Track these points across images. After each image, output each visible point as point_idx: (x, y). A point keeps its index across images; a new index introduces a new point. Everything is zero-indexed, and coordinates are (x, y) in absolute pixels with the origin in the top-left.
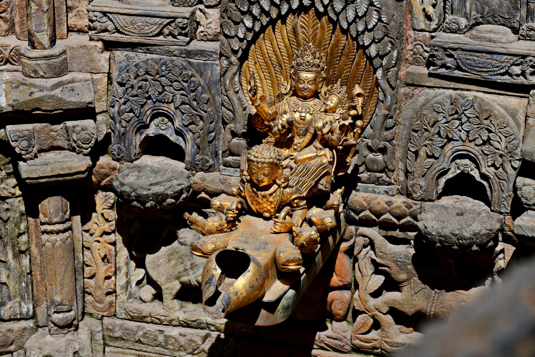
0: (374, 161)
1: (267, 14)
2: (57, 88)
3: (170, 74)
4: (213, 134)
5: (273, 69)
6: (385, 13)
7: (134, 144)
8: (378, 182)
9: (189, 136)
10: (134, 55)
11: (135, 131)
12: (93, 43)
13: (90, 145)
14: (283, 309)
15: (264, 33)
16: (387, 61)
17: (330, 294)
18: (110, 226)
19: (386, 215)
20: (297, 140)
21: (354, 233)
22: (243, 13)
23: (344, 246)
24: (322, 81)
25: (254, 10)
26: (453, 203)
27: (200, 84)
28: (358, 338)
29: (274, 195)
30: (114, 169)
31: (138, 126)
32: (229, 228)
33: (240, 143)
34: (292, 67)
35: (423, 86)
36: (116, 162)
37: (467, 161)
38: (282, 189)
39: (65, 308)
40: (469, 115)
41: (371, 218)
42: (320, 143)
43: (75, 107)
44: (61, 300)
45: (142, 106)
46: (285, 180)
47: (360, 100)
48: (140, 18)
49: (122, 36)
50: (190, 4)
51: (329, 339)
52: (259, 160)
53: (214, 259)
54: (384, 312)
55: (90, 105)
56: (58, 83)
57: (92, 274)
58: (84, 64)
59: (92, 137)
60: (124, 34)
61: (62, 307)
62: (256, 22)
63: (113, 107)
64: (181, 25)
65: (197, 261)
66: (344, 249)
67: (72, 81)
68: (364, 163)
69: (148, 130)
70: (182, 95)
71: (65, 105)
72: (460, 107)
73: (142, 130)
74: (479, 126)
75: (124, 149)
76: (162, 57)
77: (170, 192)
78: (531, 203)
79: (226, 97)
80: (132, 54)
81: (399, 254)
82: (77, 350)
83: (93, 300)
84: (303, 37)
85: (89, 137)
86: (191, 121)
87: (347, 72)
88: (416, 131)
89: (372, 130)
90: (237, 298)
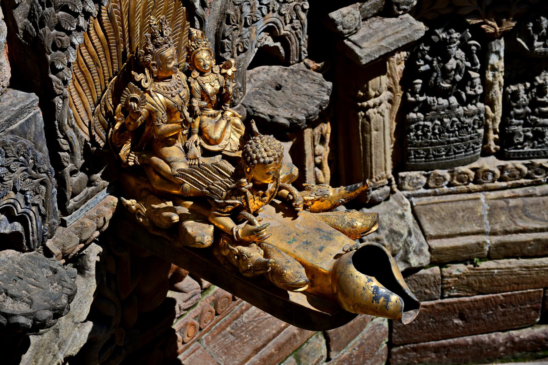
5: (89, 74)
9: (32, 212)
34: (147, 53)
42: (214, 109)
79: (62, 140)
88: (228, 38)
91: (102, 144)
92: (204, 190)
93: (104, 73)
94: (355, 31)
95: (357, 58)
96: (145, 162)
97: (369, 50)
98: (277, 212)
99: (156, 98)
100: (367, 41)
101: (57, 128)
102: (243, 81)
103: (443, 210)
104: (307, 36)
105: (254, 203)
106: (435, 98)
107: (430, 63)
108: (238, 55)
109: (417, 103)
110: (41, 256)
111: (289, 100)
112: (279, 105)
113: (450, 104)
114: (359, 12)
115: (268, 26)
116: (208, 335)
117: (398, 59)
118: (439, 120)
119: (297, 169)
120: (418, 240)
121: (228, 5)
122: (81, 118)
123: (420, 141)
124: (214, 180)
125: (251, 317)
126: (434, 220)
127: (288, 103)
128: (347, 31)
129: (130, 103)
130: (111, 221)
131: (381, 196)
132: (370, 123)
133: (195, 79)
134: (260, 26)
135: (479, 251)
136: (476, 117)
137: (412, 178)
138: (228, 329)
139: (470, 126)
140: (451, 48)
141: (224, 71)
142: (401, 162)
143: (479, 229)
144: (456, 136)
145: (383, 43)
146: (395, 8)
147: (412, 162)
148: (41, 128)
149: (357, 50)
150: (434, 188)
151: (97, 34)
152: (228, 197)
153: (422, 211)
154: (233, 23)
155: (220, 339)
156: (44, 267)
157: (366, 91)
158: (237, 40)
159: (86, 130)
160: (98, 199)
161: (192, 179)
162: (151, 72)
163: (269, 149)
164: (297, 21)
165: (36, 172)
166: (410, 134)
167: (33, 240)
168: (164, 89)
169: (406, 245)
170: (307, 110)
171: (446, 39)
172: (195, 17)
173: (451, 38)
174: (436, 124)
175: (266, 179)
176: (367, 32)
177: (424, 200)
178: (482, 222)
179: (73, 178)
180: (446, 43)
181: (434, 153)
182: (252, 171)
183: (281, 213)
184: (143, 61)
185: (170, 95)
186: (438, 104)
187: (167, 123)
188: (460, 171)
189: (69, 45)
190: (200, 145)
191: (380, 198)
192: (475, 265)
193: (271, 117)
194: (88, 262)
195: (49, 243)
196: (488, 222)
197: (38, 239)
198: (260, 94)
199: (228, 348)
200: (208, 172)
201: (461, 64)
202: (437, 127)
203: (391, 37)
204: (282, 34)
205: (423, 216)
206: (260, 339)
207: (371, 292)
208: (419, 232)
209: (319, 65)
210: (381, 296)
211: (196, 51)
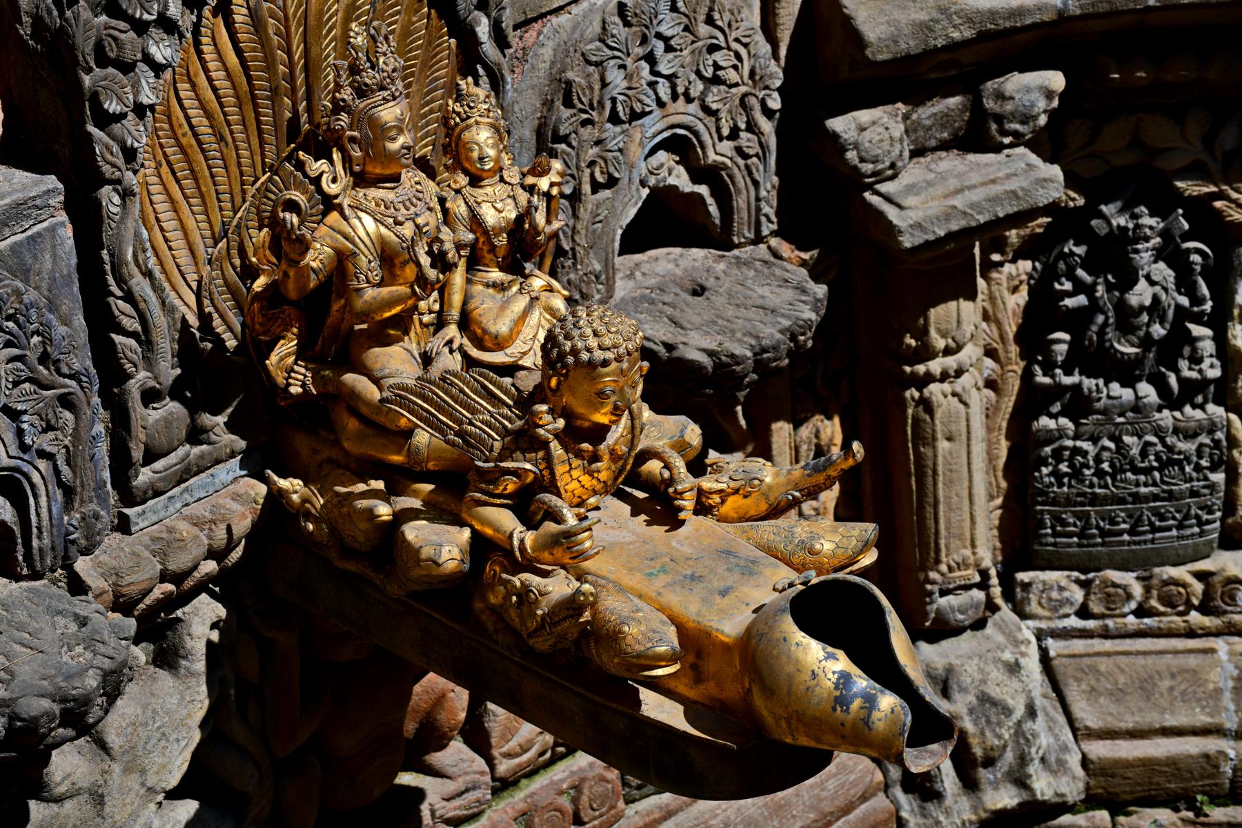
9: (39, 473)
17: (417, 688)
26: (631, 284)
28: (509, 755)
35: (543, 16)
37: (662, 156)
40: (669, 33)
42: (501, 270)
52: (622, 350)
53: (800, 636)
65: (117, 818)
72: (648, 24)
74: (690, 48)
78: (887, 164)
79: (120, 302)
88: (565, 139)
91: (231, 343)
92: (451, 437)
93: (239, 164)
94: (890, 172)
95: (891, 230)
96: (330, 389)
97: (921, 214)
98: (634, 513)
99: (355, 222)
100: (917, 194)
101: (108, 267)
102: (607, 259)
103: (1122, 671)
104: (775, 179)
105: (572, 478)
106: (1101, 382)
107: (1089, 290)
108: (594, 191)
109: (1058, 390)
110: (64, 593)
111: (717, 316)
112: (693, 324)
113: (1138, 398)
114: (902, 127)
115: (675, 135)
117: (1010, 277)
118: (1111, 438)
119: (698, 431)
120: (1056, 737)
121: (569, 60)
122: (178, 266)
123: (1065, 489)
124: (473, 411)
126: (1100, 694)
127: (715, 323)
128: (871, 166)
129: (281, 215)
130: (249, 537)
131: (962, 613)
132: (932, 418)
133: (458, 191)
134: (653, 130)
135: (1209, 777)
136: (1205, 439)
137: (1047, 587)
139: (1188, 459)
140: (1137, 251)
141: (530, 180)
142: (1022, 545)
143: (1209, 720)
144: (1155, 484)
145: (958, 202)
146: (994, 127)
147: (1047, 545)
148: (68, 266)
149: (892, 213)
150: (1102, 617)
151: (221, 58)
152: (506, 454)
153: (1070, 671)
154: (580, 106)
156: (59, 613)
157: (922, 334)
158: (592, 152)
159: (191, 299)
160: (217, 480)
161: (422, 408)
162: (347, 160)
163: (604, 331)
164: (750, 135)
165: (48, 369)
166: (1040, 471)
167: (40, 549)
168: (377, 205)
169: (1022, 741)
170: (757, 337)
171: (1123, 230)
172: (479, 67)
173: (1137, 226)
174: (1104, 448)
175: (597, 410)
176: (921, 179)
177: (1079, 645)
178: (1217, 706)
179: (151, 412)
180: (1125, 241)
181: (1102, 524)
182: (564, 387)
183: (643, 517)
184: (329, 129)
185: (391, 220)
186: (1109, 397)
187: (379, 285)
188: (1165, 577)
189: (139, 56)
190: (461, 348)
191: (960, 617)
192: (1199, 812)
193: (669, 347)
194: (187, 639)
195: (82, 565)
196: (1232, 707)
197: (53, 549)
198: (652, 302)
200: (462, 391)
201: (1164, 296)
202: (1106, 455)
203: (977, 190)
204: (710, 161)
205: (1071, 681)
207: (830, 684)
208: (1062, 719)
209: (806, 256)
210: (856, 696)
211: (462, 125)
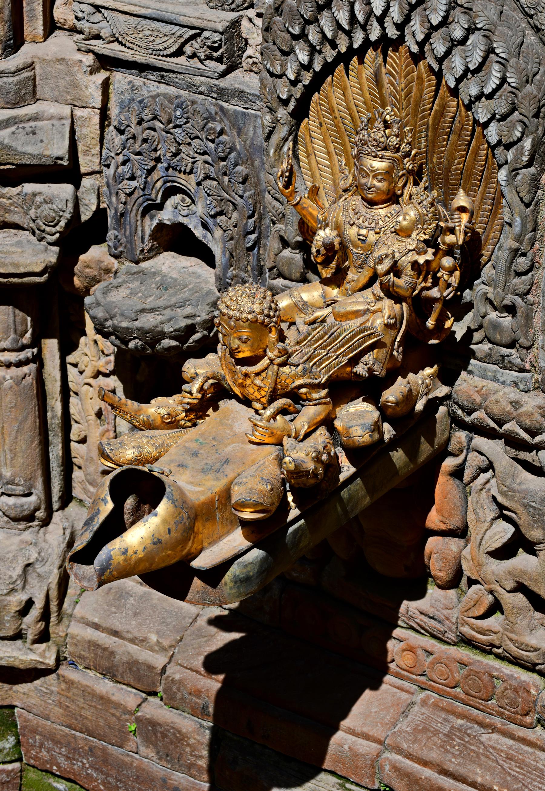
0: (496, 326)
1: (334, 45)
2: (6, 127)
3: (189, 125)
4: (253, 237)
6: (513, 70)
7: (140, 233)
8: (504, 363)
10: (141, 83)
11: (140, 212)
12: (79, 56)
13: (58, 228)
14: (235, 582)
15: (333, 76)
16: (515, 156)
18: (108, 363)
19: (511, 424)
20: (351, 275)
21: (465, 444)
22: (295, 38)
23: (449, 463)
24: (403, 175)
25: (310, 34)
27: (232, 149)
29: (264, 375)
30: (108, 271)
31: (145, 204)
32: (189, 421)
33: (293, 259)
36: (113, 260)
38: (276, 367)
39: (19, 490)
41: (488, 425)
43: (34, 162)
44: (12, 475)
45: (150, 172)
46: (280, 352)
47: (465, 217)
48: (149, 22)
49: (123, 48)
50: (233, 6)
51: (422, 617)
52: (231, 313)
54: (508, 589)
55: (60, 162)
56: (8, 120)
57: (82, 436)
58: (61, 89)
59: (61, 217)
60: (125, 45)
61: (14, 487)
62: (316, 54)
63: (108, 166)
64: (209, 43)
66: (449, 469)
67: (36, 118)
68: (481, 327)
69: (162, 212)
70: (206, 162)
71: (17, 157)
73: (153, 212)
75: (123, 240)
76: (182, 92)
77: (168, 328)
80: (138, 81)
81: (532, 494)
82: (31, 561)
83: (84, 478)
84: (391, 91)
85: (54, 215)
86: (218, 209)
87: (459, 164)
89: (494, 271)
90: (125, 560)
116: (434, 697)
125: (491, 743)
138: (460, 722)
155: (440, 717)
199: (425, 730)
206: (459, 764)
